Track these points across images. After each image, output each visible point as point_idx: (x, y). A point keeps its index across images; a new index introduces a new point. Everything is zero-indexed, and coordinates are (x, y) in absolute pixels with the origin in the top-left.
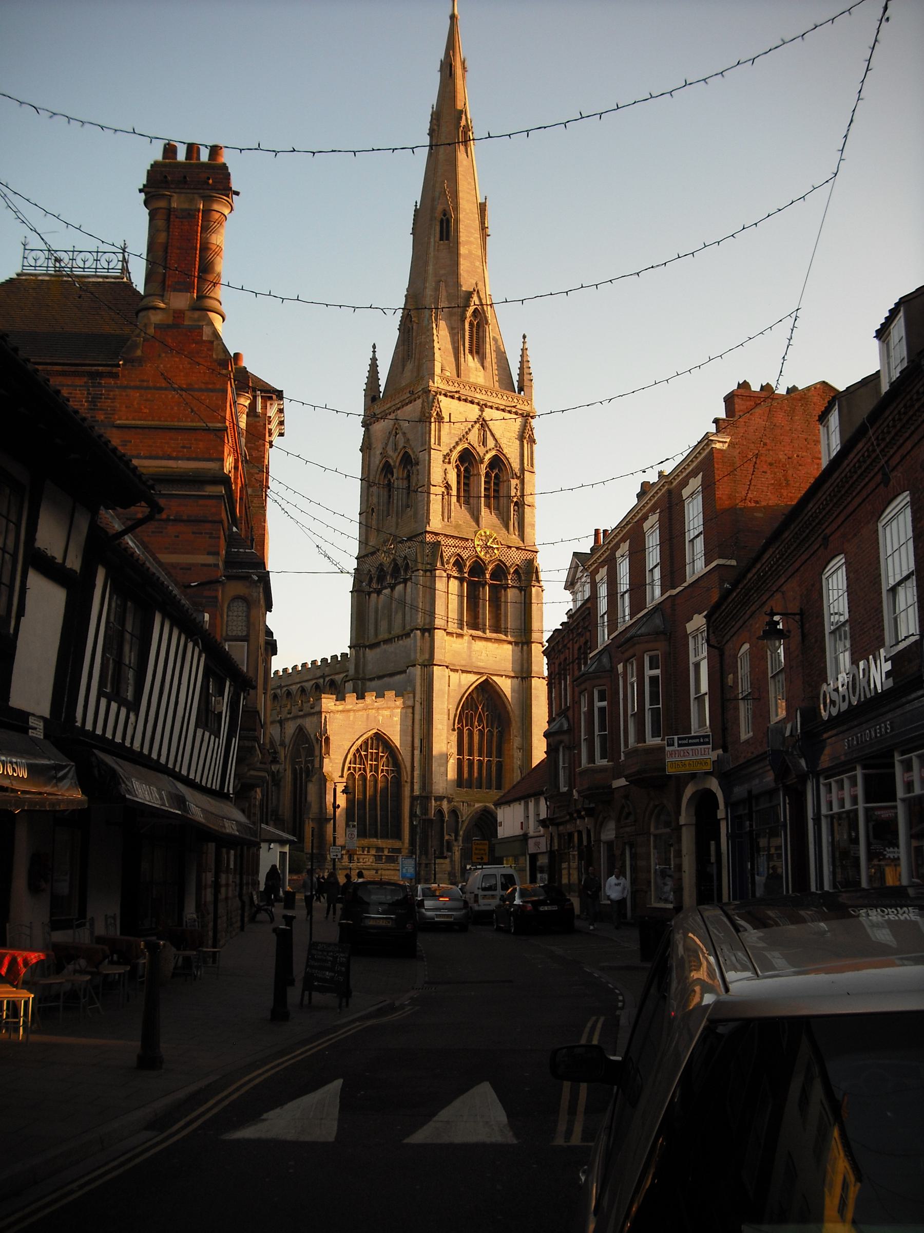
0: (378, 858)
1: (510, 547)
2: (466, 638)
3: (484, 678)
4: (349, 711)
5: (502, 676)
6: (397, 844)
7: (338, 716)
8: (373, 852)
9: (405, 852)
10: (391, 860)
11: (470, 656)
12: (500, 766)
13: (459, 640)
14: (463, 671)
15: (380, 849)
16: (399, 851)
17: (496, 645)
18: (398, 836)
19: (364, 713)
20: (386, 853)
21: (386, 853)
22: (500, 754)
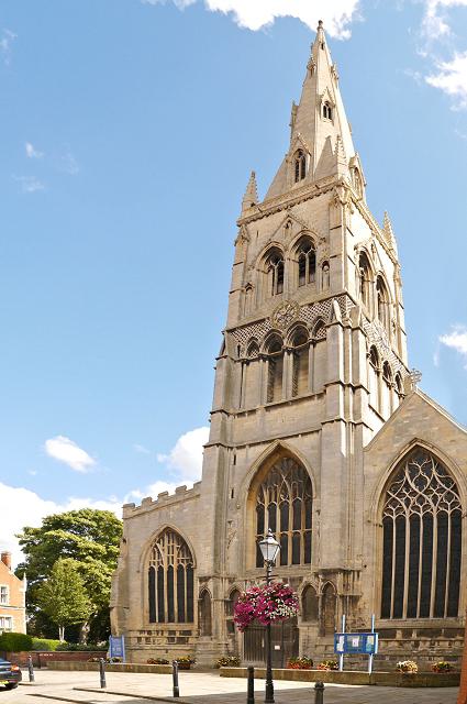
0: (171, 640)
1: (311, 304)
2: (259, 412)
3: (275, 445)
4: (143, 513)
5: (297, 436)
6: (185, 626)
7: (136, 520)
8: (166, 634)
9: (194, 634)
10: (182, 641)
11: (263, 429)
12: (308, 536)
13: (252, 417)
14: (251, 445)
15: (173, 632)
16: (189, 633)
17: (294, 407)
18: (191, 620)
19: (157, 513)
20: (178, 635)
21: (178, 635)
22: (309, 525)
